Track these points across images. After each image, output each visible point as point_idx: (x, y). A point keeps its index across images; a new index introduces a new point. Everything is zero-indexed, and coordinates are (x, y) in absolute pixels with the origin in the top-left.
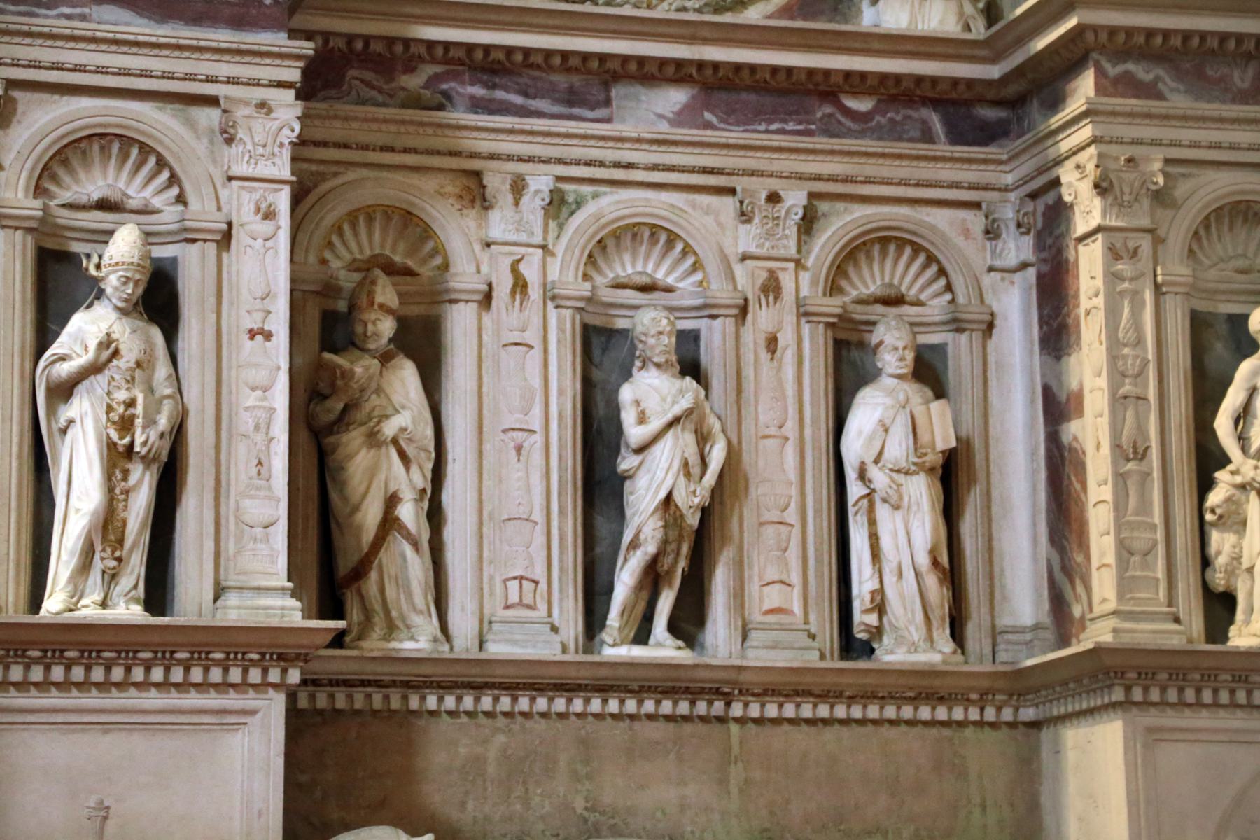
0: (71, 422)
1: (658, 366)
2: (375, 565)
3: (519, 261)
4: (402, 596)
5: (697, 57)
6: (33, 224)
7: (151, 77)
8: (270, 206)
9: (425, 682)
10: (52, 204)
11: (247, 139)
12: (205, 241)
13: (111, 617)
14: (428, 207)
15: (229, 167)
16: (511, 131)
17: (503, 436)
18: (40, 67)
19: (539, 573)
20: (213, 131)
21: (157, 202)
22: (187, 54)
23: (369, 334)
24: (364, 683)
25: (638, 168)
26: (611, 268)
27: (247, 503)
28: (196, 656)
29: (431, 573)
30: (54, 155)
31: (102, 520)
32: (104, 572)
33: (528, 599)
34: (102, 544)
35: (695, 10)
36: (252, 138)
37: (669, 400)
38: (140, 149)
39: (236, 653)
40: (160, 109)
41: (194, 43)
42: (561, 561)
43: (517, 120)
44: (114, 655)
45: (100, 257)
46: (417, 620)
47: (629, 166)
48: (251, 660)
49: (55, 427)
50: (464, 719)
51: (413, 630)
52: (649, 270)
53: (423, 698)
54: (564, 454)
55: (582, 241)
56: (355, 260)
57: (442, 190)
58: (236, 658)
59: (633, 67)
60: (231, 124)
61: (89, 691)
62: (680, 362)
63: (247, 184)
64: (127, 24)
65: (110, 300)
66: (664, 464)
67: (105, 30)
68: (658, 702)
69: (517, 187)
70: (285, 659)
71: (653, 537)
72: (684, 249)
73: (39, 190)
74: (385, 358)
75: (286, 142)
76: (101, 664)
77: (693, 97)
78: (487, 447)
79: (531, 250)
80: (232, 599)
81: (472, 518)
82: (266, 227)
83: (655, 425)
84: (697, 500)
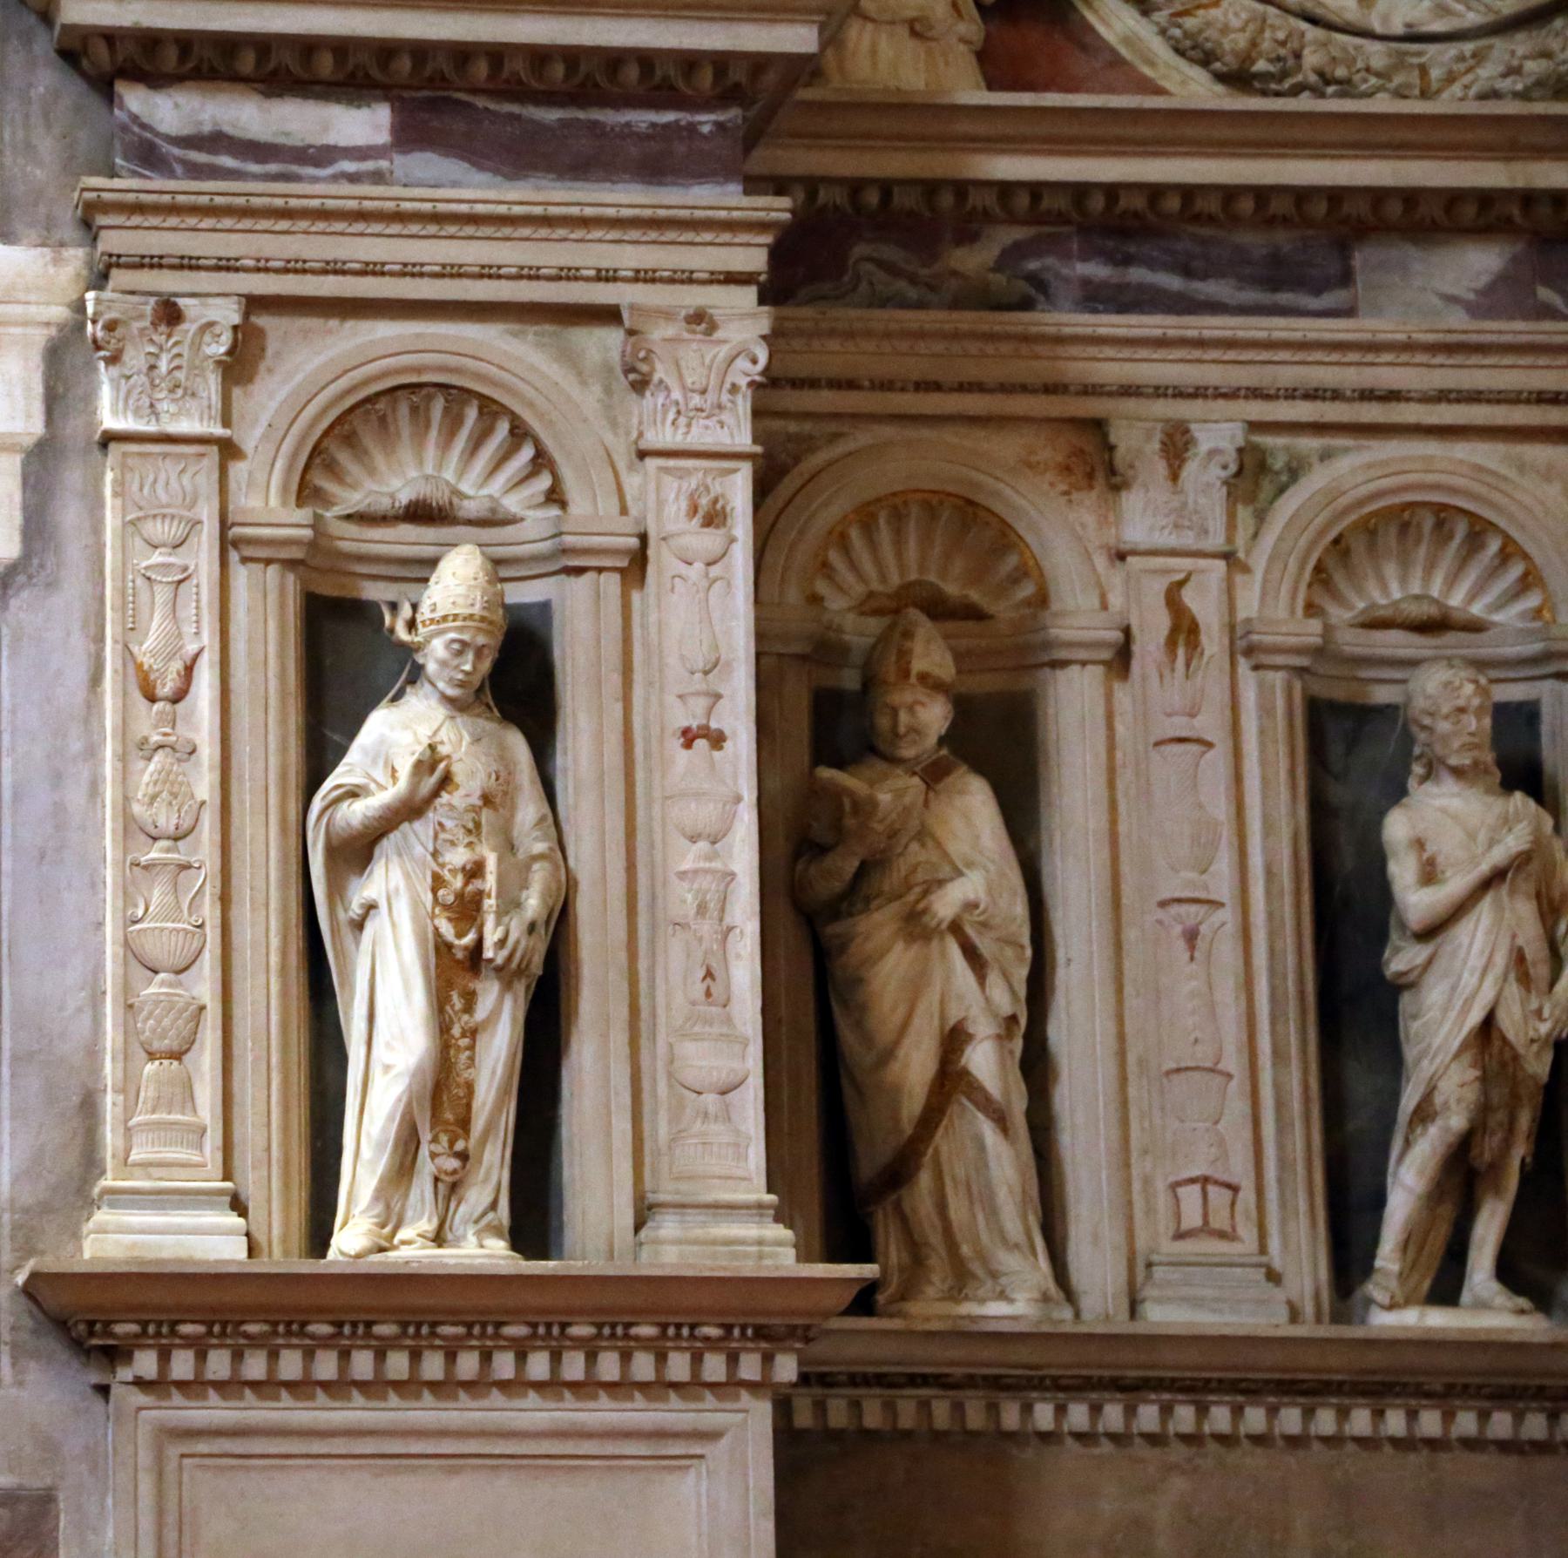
0: (371, 907)
1: (1458, 773)
2: (927, 1159)
3: (1181, 584)
4: (980, 1217)
5: (1520, 183)
6: (296, 553)
7: (499, 277)
8: (715, 501)
9: (1030, 1379)
10: (328, 514)
11: (671, 382)
12: (600, 570)
13: (452, 1261)
14: (1008, 491)
15: (641, 435)
16: (1162, 343)
17: (1160, 914)
18: (304, 271)
19: (1239, 1168)
20: (610, 370)
21: (512, 503)
22: (561, 232)
23: (902, 730)
24: (914, 1380)
25: (1408, 400)
26: (1360, 591)
27: (689, 1049)
28: (606, 1331)
29: (1033, 1173)
30: (332, 427)
31: (430, 1085)
32: (436, 1180)
33: (1219, 1221)
34: (432, 1129)
35: (1517, 95)
36: (681, 377)
37: (1482, 837)
39: (679, 1326)
40: (515, 335)
41: (575, 211)
42: (1281, 1147)
43: (1171, 320)
44: (461, 1330)
45: (415, 607)
46: (1009, 1261)
47: (1393, 396)
48: (707, 1339)
49: (341, 915)
50: (1107, 1447)
51: (1003, 1280)
52: (1435, 591)
53: (1027, 1409)
54: (1279, 945)
55: (1303, 542)
56: (871, 595)
57: (1034, 459)
58: (678, 1336)
59: (1394, 209)
60: (642, 354)
61: (418, 1397)
62: (1501, 763)
63: (671, 463)
64: (455, 184)
65: (433, 685)
66: (1476, 961)
67: (414, 198)
68: (1484, 1416)
69: (1174, 444)
70: (768, 1337)
71: (1459, 1101)
72: (1502, 550)
73: (306, 493)
74: (934, 774)
75: (743, 382)
76: (440, 1347)
77: (1515, 260)
78: (1131, 934)
79: (1202, 563)
80: (667, 1227)
81: (1105, 1071)
82: (710, 541)
83: (1456, 885)
84: (1544, 1028)
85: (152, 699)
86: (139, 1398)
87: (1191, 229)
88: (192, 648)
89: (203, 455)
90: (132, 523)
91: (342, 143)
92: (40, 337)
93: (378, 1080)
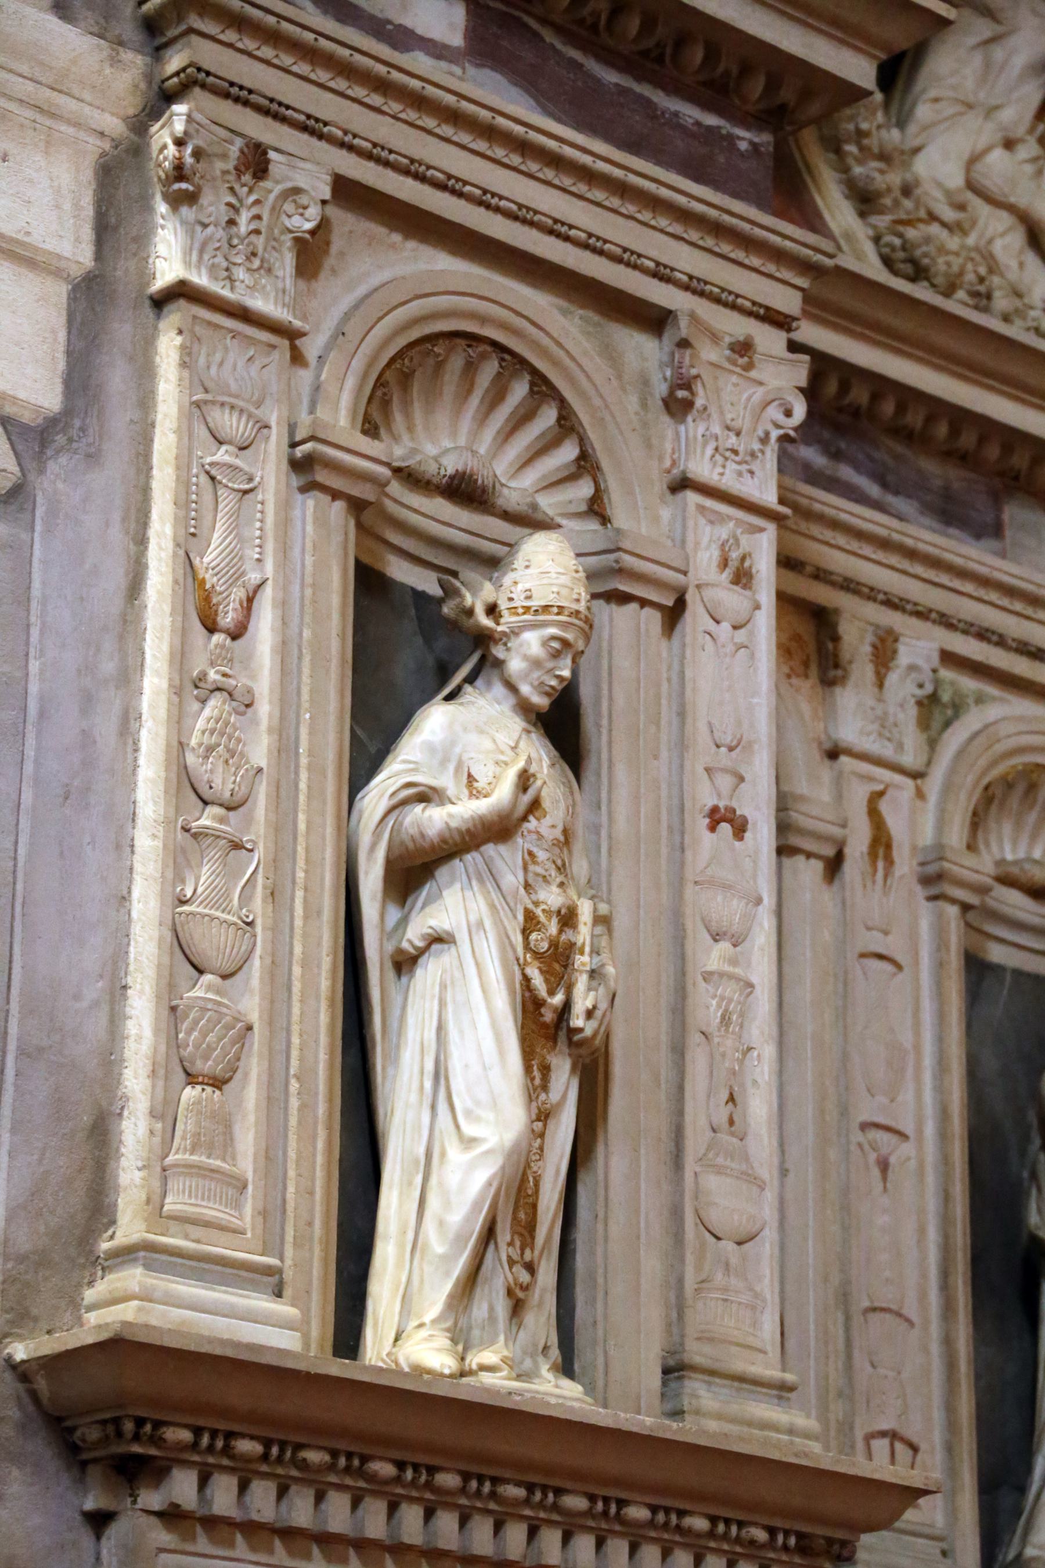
0: (438, 939)
3: (881, 794)
8: (743, 559)
12: (644, 603)
17: (857, 1136)
21: (548, 503)
38: (532, 384)
40: (565, 313)
63: (709, 503)
65: (512, 687)
75: (775, 434)
79: (898, 778)
82: (732, 600)
85: (211, 628)
86: (162, 1536)
87: (890, 443)
88: (253, 577)
89: (274, 347)
90: (198, 405)
91: (419, 31)
92: (94, 147)
93: (456, 1155)
